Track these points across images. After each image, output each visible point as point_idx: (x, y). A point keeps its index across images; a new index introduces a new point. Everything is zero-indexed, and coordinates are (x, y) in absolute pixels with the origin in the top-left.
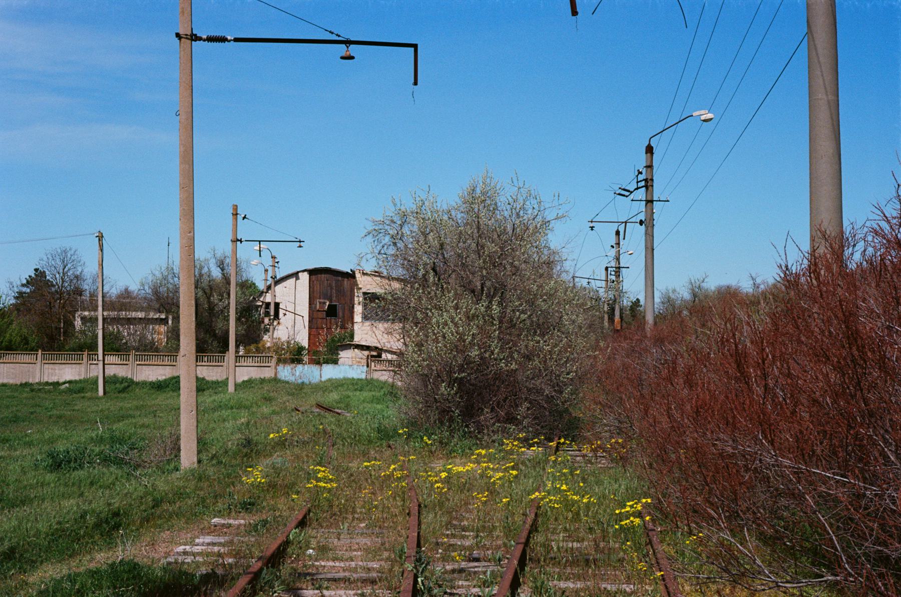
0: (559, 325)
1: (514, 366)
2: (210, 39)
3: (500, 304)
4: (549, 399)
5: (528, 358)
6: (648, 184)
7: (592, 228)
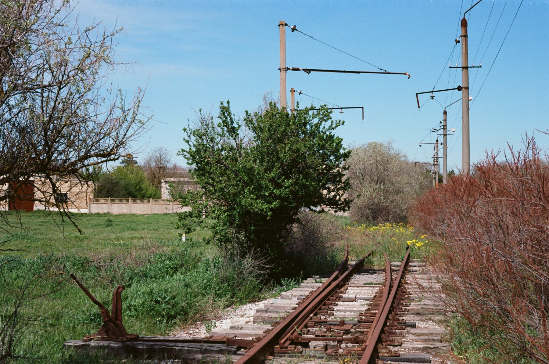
0: (402, 192)
1: (388, 204)
2: (294, 69)
3: (384, 185)
4: (399, 215)
5: (392, 202)
6: (445, 128)
7: (420, 146)
